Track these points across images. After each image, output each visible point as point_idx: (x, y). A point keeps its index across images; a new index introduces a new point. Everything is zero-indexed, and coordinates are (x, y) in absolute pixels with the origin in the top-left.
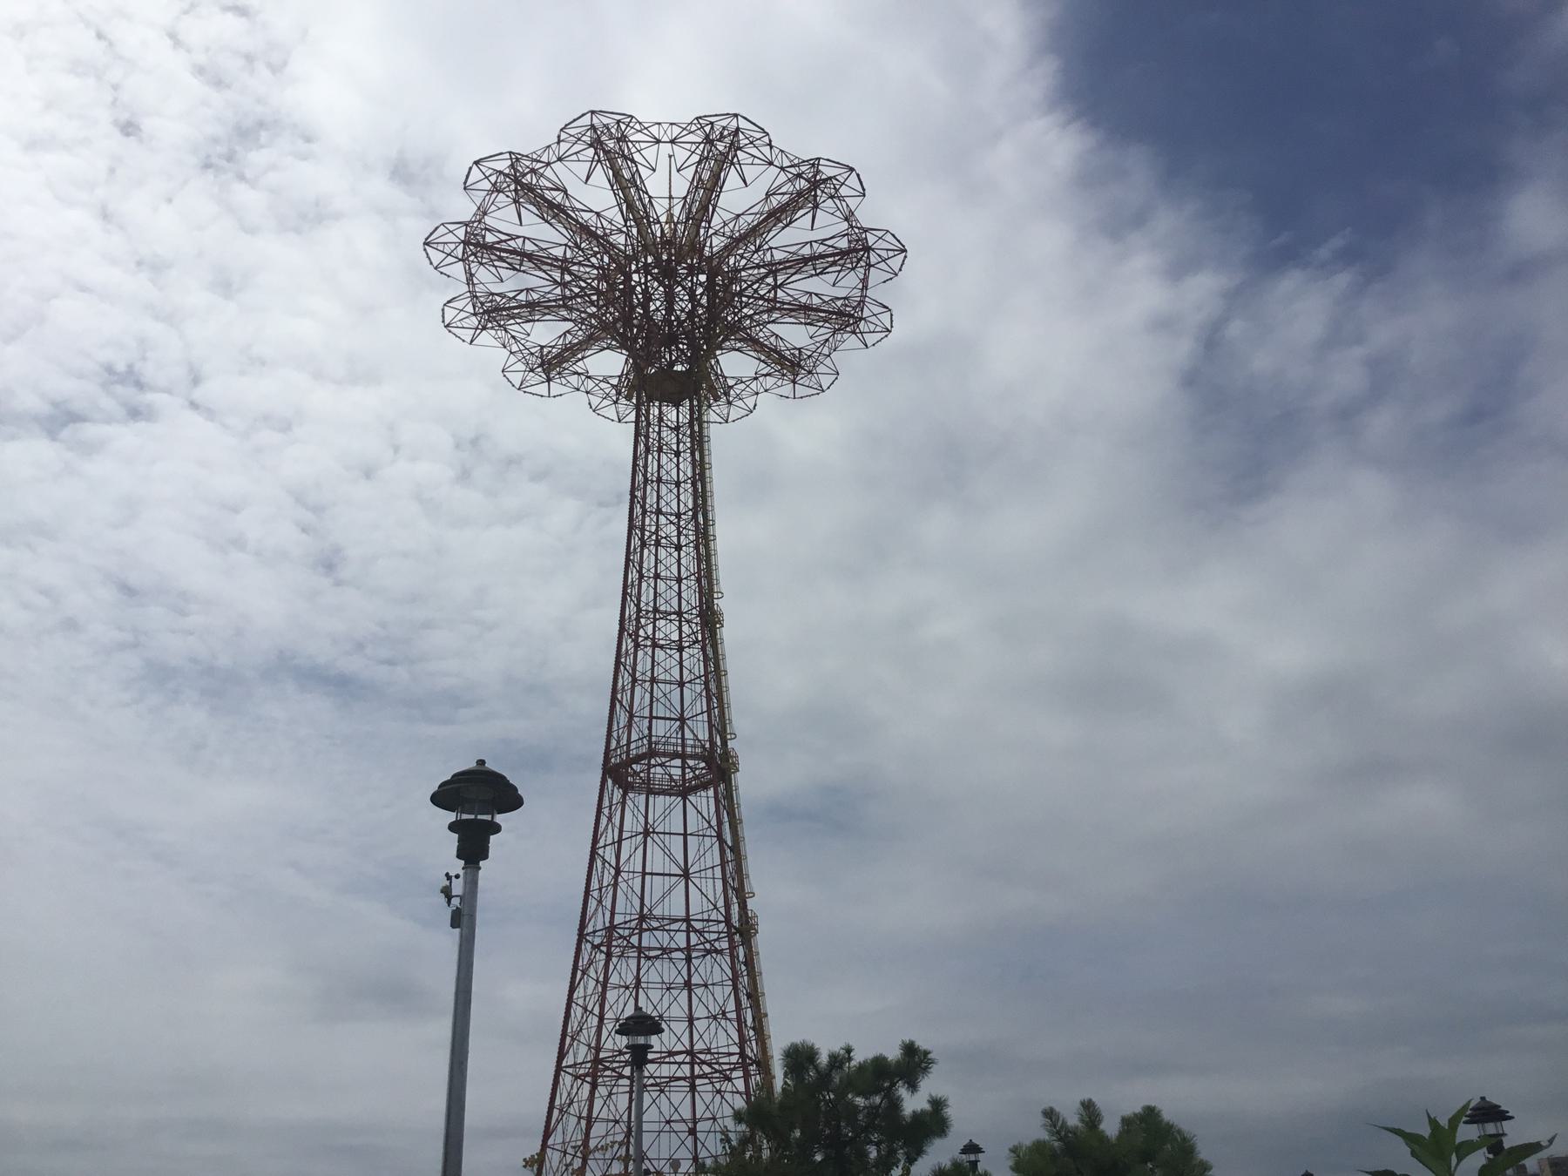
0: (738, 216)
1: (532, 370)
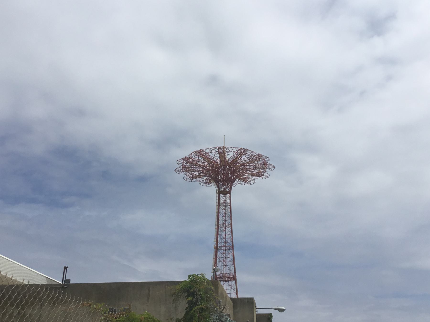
1: (190, 178)
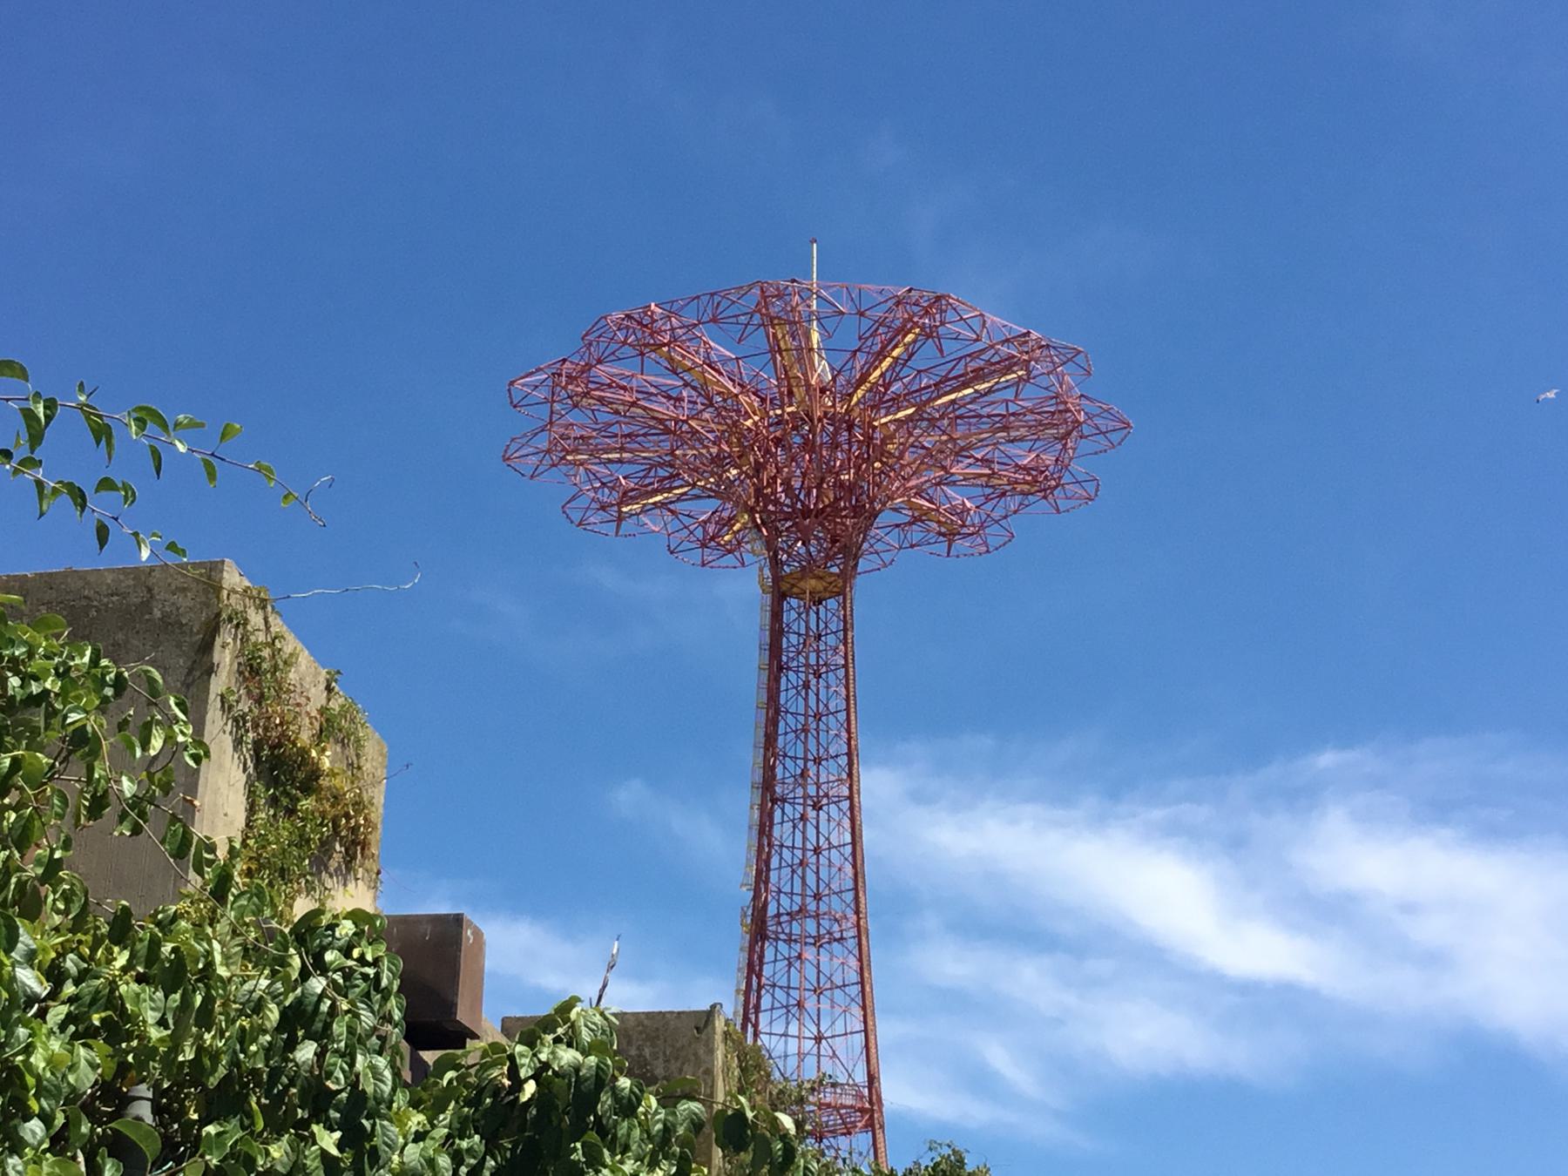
1: (603, 508)
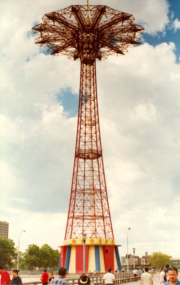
0: (105, 21)
